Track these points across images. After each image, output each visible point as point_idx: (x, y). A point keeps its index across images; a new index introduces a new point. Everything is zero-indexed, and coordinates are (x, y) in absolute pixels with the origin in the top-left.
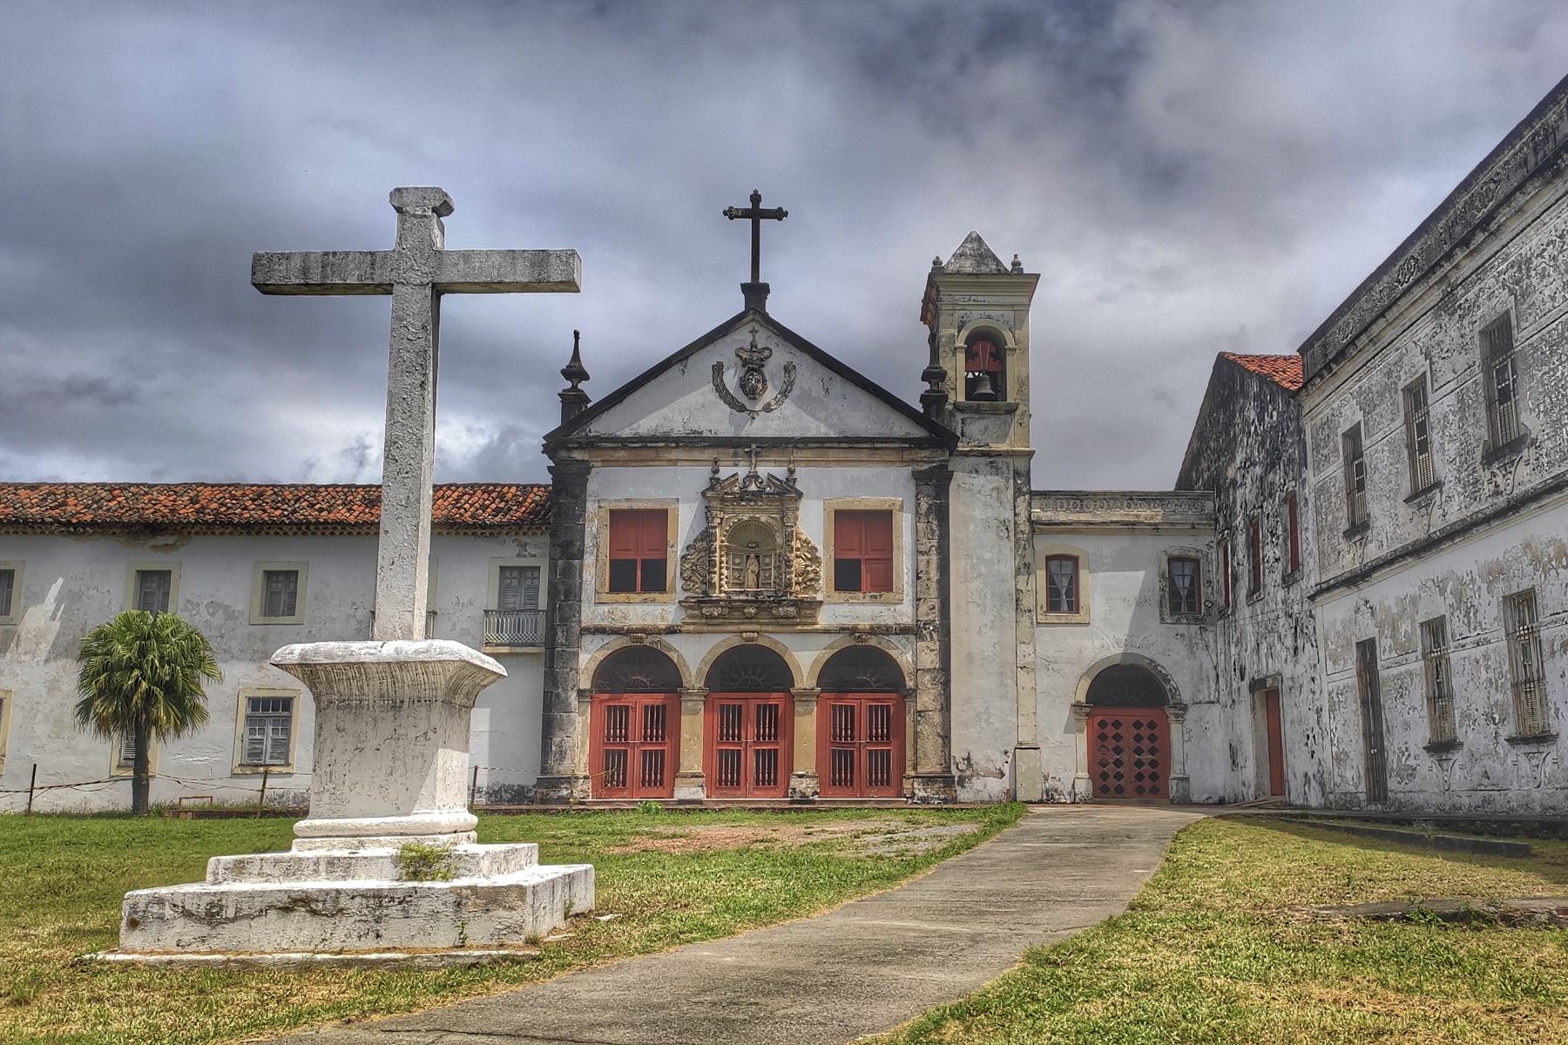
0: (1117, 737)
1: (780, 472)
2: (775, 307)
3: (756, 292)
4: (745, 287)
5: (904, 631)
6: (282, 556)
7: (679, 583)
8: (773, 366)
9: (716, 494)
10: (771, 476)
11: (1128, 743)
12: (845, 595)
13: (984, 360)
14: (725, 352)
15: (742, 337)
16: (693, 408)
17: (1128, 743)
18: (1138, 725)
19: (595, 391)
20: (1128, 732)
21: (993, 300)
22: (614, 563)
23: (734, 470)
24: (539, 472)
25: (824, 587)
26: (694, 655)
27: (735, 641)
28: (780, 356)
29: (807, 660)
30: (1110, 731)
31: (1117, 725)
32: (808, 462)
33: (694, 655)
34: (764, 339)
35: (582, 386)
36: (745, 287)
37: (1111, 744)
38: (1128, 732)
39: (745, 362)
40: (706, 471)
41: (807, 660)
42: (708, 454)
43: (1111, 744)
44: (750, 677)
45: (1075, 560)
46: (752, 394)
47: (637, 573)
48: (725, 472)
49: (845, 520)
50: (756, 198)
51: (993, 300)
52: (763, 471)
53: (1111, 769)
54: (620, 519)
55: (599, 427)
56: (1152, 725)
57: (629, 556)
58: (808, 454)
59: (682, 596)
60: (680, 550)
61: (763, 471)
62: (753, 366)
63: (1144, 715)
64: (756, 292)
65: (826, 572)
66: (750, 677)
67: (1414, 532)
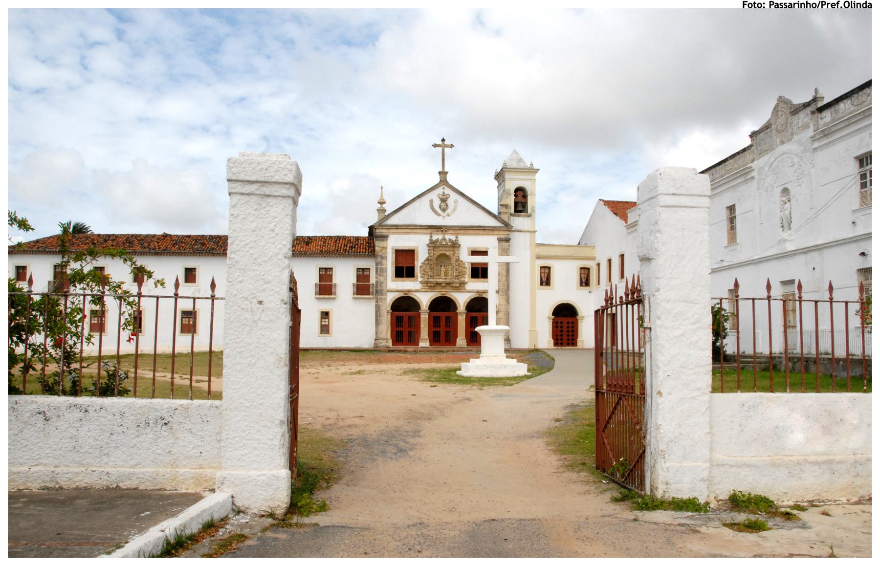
1: (453, 238)
2: (450, 179)
3: (443, 174)
4: (440, 173)
7: (419, 275)
8: (450, 202)
9: (433, 245)
10: (450, 240)
11: (565, 329)
14: (435, 196)
15: (440, 191)
16: (422, 214)
17: (565, 329)
18: (568, 323)
19: (389, 208)
20: (565, 325)
22: (396, 268)
24: (365, 233)
26: (425, 299)
27: (439, 295)
28: (453, 196)
29: (461, 299)
31: (561, 323)
32: (462, 234)
33: (425, 299)
34: (448, 191)
35: (384, 206)
36: (440, 173)
38: (565, 325)
41: (461, 299)
42: (429, 231)
44: (443, 305)
45: (549, 268)
46: (444, 210)
47: (404, 270)
48: (435, 238)
50: (443, 140)
52: (447, 237)
53: (559, 337)
54: (399, 253)
55: (390, 222)
58: (462, 232)
59: (420, 279)
61: (447, 237)
62: (444, 200)
63: (570, 319)
64: (443, 174)
66: (443, 305)
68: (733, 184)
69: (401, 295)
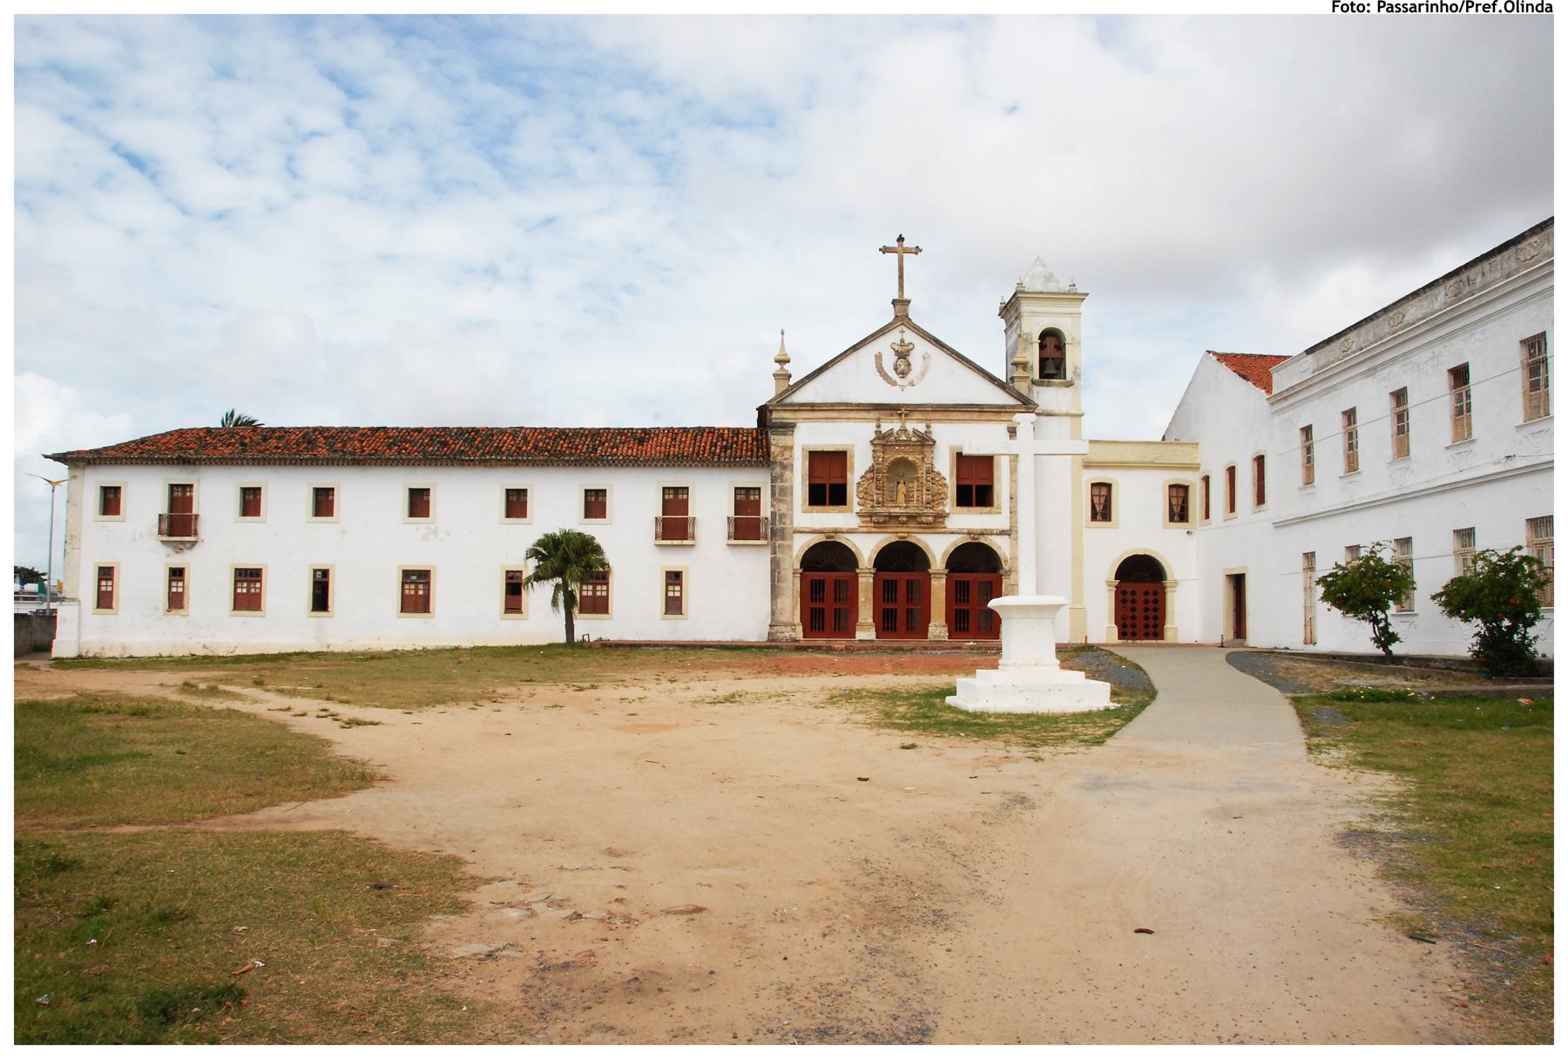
0: (1133, 601)
1: (921, 428)
2: (914, 313)
3: (901, 303)
4: (894, 302)
5: (1002, 533)
6: (596, 478)
7: (856, 500)
8: (915, 358)
9: (882, 442)
10: (915, 432)
11: (1140, 606)
12: (965, 509)
13: (1051, 352)
14: (885, 346)
15: (894, 337)
16: (861, 382)
17: (1140, 606)
18: (1146, 593)
19: (797, 372)
20: (1140, 598)
21: (1044, 309)
22: (811, 486)
23: (891, 425)
24: (752, 423)
25: (949, 505)
26: (867, 547)
27: (893, 538)
28: (921, 347)
29: (938, 547)
30: (1129, 597)
31: (1133, 593)
32: (939, 420)
33: (867, 547)
34: (910, 337)
35: (787, 366)
36: (894, 302)
37: (1129, 605)
38: (1140, 598)
39: (897, 352)
40: (872, 427)
41: (938, 547)
42: (874, 415)
43: (1129, 605)
44: (901, 560)
45: (1109, 486)
46: (903, 374)
48: (885, 427)
49: (962, 460)
50: (901, 239)
51: (1044, 309)
52: (910, 426)
53: (1129, 622)
54: (816, 457)
55: (800, 397)
56: (1155, 593)
57: (968, 483)
58: (938, 416)
59: (857, 508)
60: (857, 479)
61: (910, 426)
62: (903, 354)
63: (1150, 587)
64: (901, 303)
65: (951, 492)
66: (901, 560)
67: (1446, 473)
68: (1499, 306)
69: (821, 538)
